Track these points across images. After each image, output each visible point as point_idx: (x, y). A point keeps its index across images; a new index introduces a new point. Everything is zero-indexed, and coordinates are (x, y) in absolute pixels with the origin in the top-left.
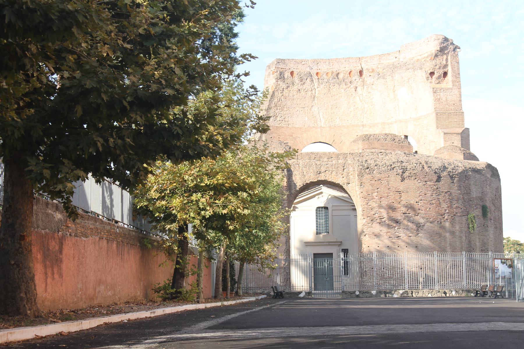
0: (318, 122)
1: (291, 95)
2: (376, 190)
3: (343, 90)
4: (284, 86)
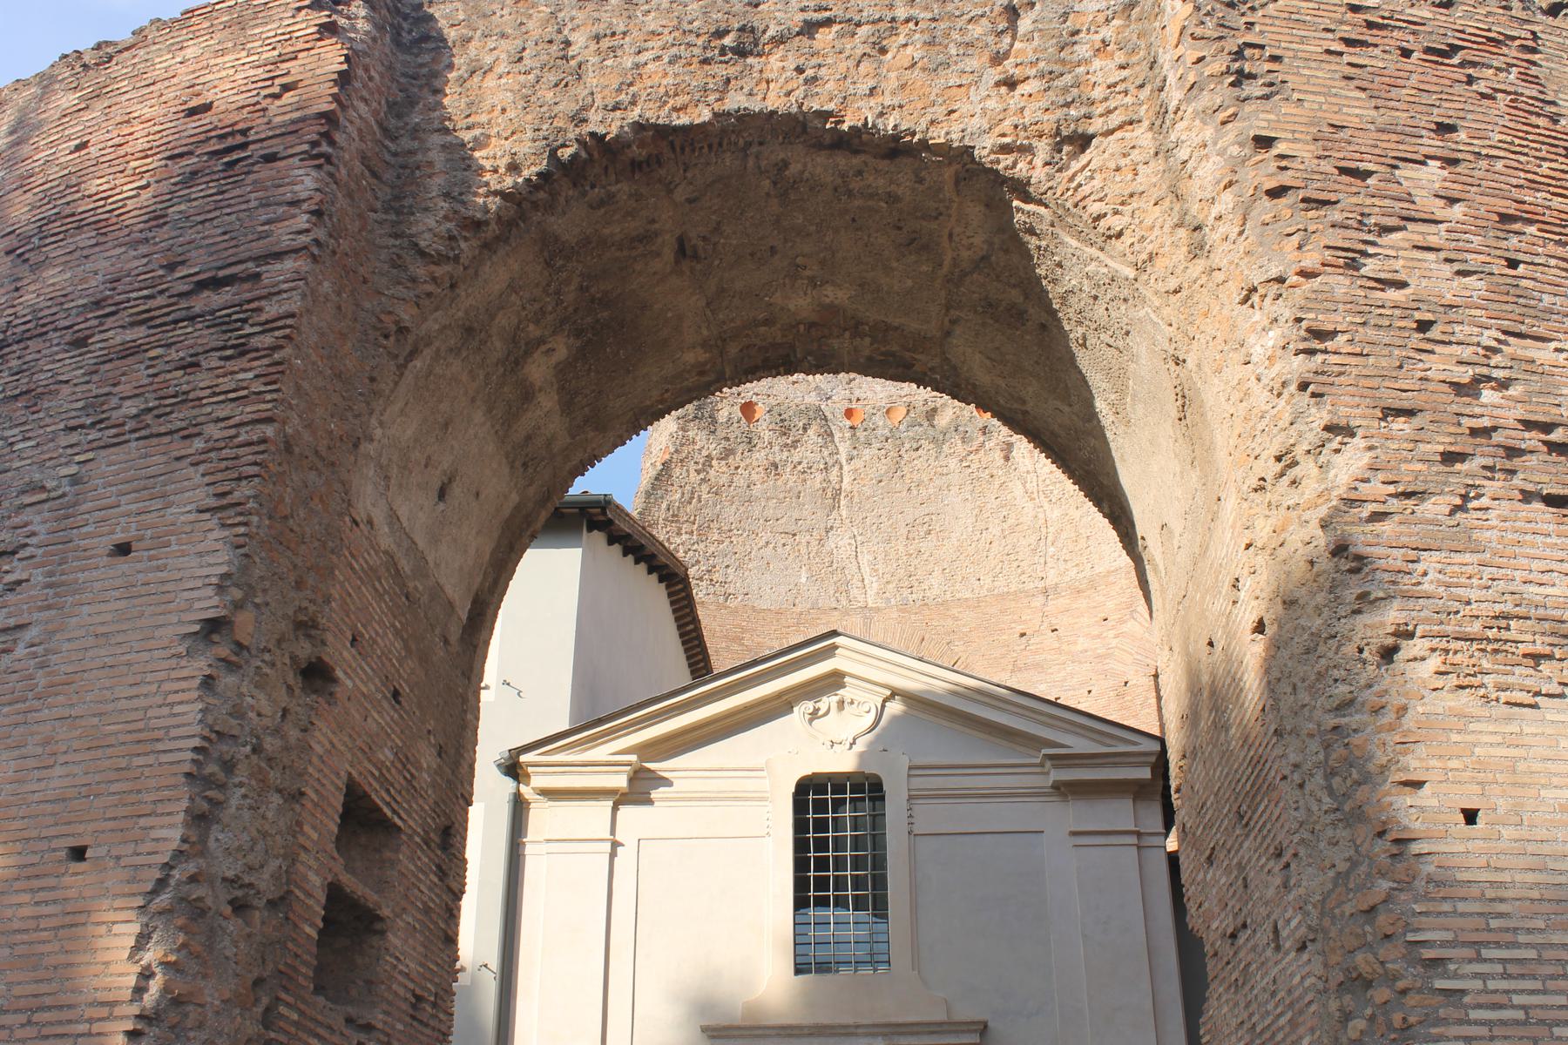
0: (854, 592)
1: (740, 481)
3: (953, 463)
4: (714, 448)
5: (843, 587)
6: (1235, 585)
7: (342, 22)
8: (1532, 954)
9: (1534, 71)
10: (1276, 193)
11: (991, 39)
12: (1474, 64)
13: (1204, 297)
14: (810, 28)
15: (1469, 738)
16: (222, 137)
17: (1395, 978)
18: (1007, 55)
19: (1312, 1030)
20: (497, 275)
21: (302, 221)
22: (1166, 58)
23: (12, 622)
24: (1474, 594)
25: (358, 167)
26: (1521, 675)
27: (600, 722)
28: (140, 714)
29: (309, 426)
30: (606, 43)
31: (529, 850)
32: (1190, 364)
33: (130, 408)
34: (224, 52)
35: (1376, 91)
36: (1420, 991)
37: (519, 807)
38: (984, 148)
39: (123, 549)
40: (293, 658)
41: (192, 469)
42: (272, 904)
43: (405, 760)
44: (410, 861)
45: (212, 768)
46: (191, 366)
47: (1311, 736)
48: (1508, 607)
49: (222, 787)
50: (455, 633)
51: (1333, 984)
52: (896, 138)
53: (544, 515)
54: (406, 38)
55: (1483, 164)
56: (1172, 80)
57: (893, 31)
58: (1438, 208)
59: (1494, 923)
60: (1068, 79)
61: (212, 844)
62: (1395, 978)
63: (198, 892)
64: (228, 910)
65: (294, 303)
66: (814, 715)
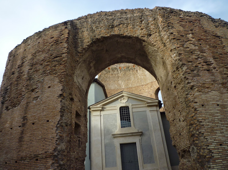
0: (122, 87)
2: (190, 32)
3: (131, 72)
5: (120, 86)
6: (171, 82)
7: (67, 27)
8: (211, 120)
9: (200, 23)
10: (174, 39)
11: (139, 24)
12: (194, 23)
13: (166, 51)
14: (119, 24)
15: (202, 97)
16: (55, 41)
17: (196, 124)
18: (141, 26)
19: (186, 130)
20: (87, 55)
21: (66, 49)
22: (159, 25)
23: (37, 96)
24: (201, 81)
25: (71, 43)
26: (206, 89)
27: (98, 102)
28: (53, 105)
29: (69, 72)
30: (97, 28)
31: (91, 117)
32: (164, 59)
33: (48, 71)
34: (54, 31)
35: (183, 26)
36: (199, 125)
37: (90, 112)
38: (140, 37)
39: (49, 87)
40: (70, 98)
41: (56, 78)
42: (70, 125)
43: (81, 108)
44: (82, 119)
45: (62, 110)
46: (55, 66)
47: (183, 98)
48: (204, 82)
49: (64, 112)
50: (85, 94)
51: (188, 125)
52: (130, 36)
53: (93, 80)
54: (74, 28)
55: (196, 34)
56: (160, 27)
57: (128, 24)
58: (192, 39)
59: (206, 117)
60: (148, 28)
61: (63, 119)
62: (196, 124)
63: (63, 124)
64: (65, 126)
65: (66, 59)
66: (121, 100)
